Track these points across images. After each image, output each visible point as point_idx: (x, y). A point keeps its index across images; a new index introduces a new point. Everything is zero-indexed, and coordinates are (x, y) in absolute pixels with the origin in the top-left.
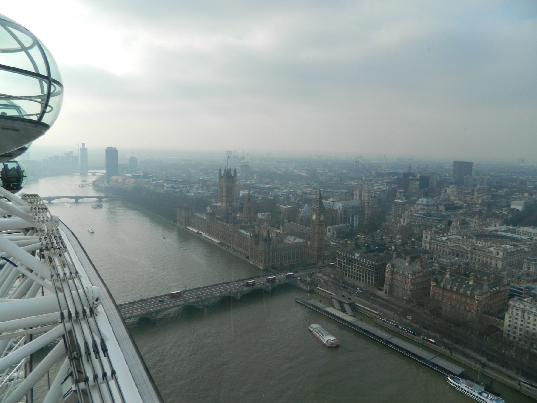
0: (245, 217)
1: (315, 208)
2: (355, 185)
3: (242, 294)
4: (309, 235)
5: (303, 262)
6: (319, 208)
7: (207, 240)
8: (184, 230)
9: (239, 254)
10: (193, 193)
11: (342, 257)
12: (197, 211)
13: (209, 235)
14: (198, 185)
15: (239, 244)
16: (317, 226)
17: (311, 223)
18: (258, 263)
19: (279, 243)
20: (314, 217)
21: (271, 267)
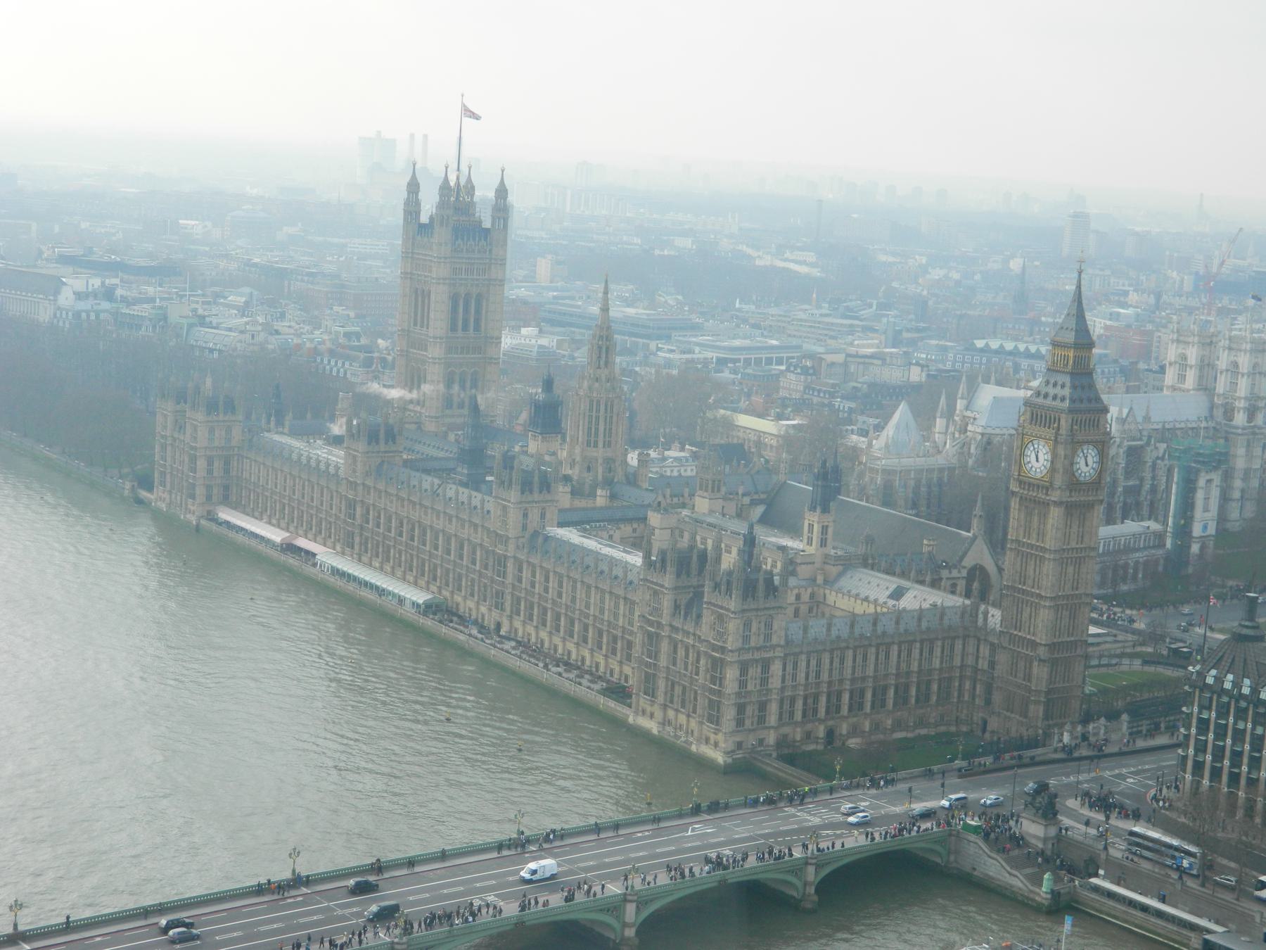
0: (578, 459)
1: (1049, 402)
2: (1107, 328)
3: (645, 914)
4: (964, 573)
5: (953, 729)
6: (1073, 401)
7: (351, 587)
8: (198, 528)
9: (560, 674)
10: (230, 330)
11: (1225, 699)
12: (280, 423)
13: (360, 560)
14: (247, 290)
15: (557, 617)
16: (1055, 514)
17: (1013, 493)
18: (693, 724)
19: (797, 613)
20: (1038, 460)
21: (774, 755)
